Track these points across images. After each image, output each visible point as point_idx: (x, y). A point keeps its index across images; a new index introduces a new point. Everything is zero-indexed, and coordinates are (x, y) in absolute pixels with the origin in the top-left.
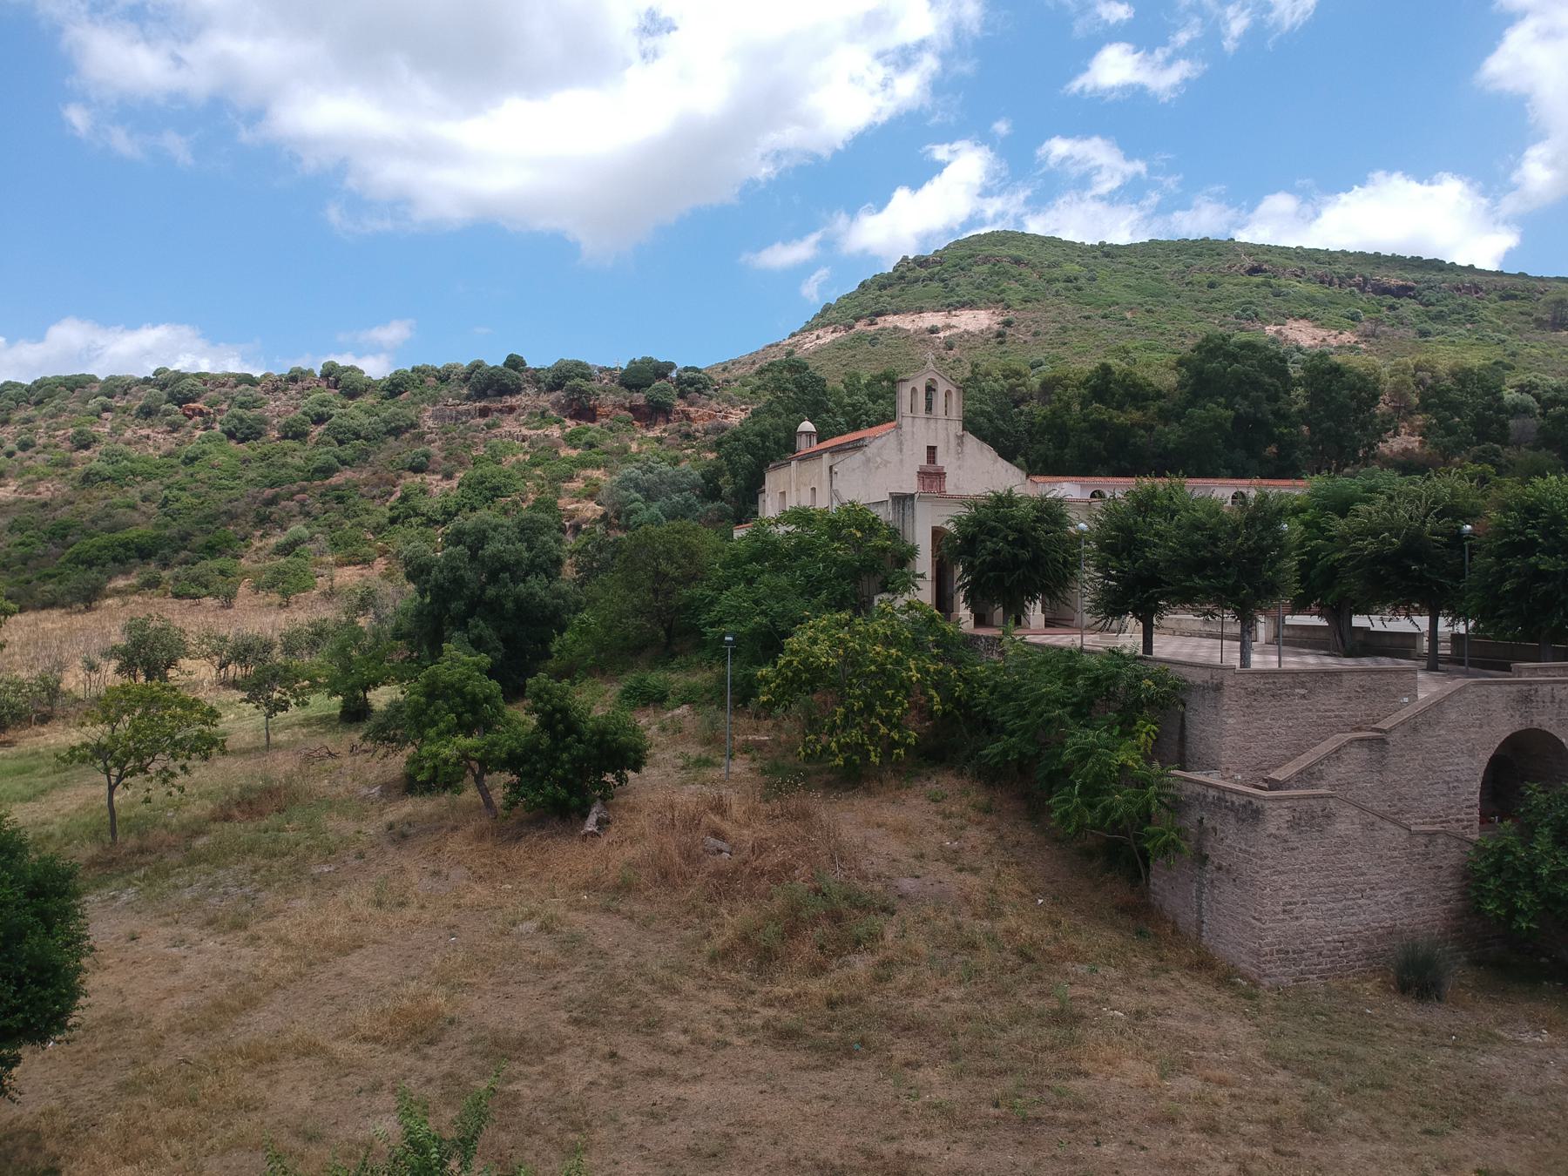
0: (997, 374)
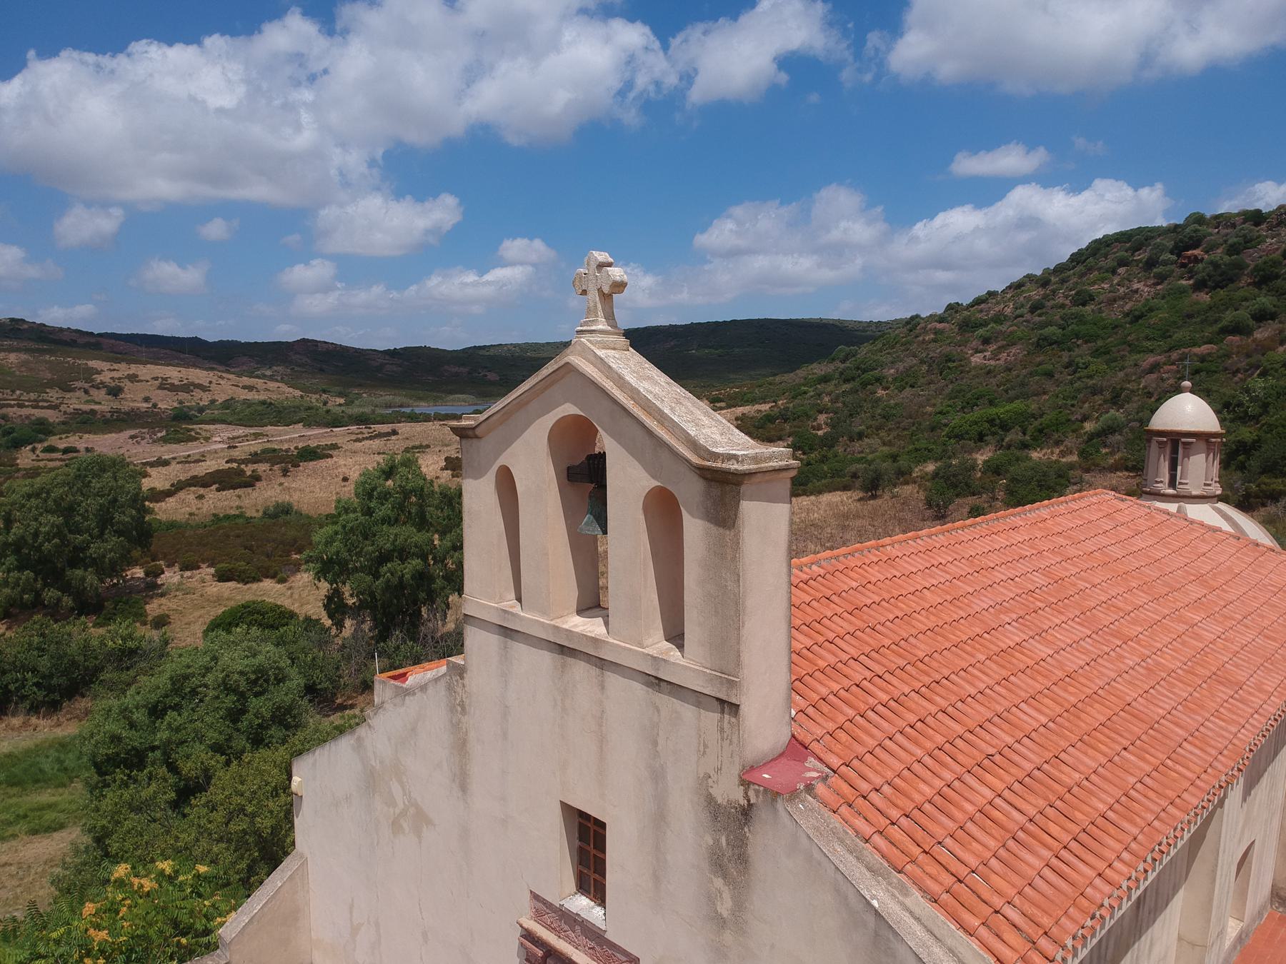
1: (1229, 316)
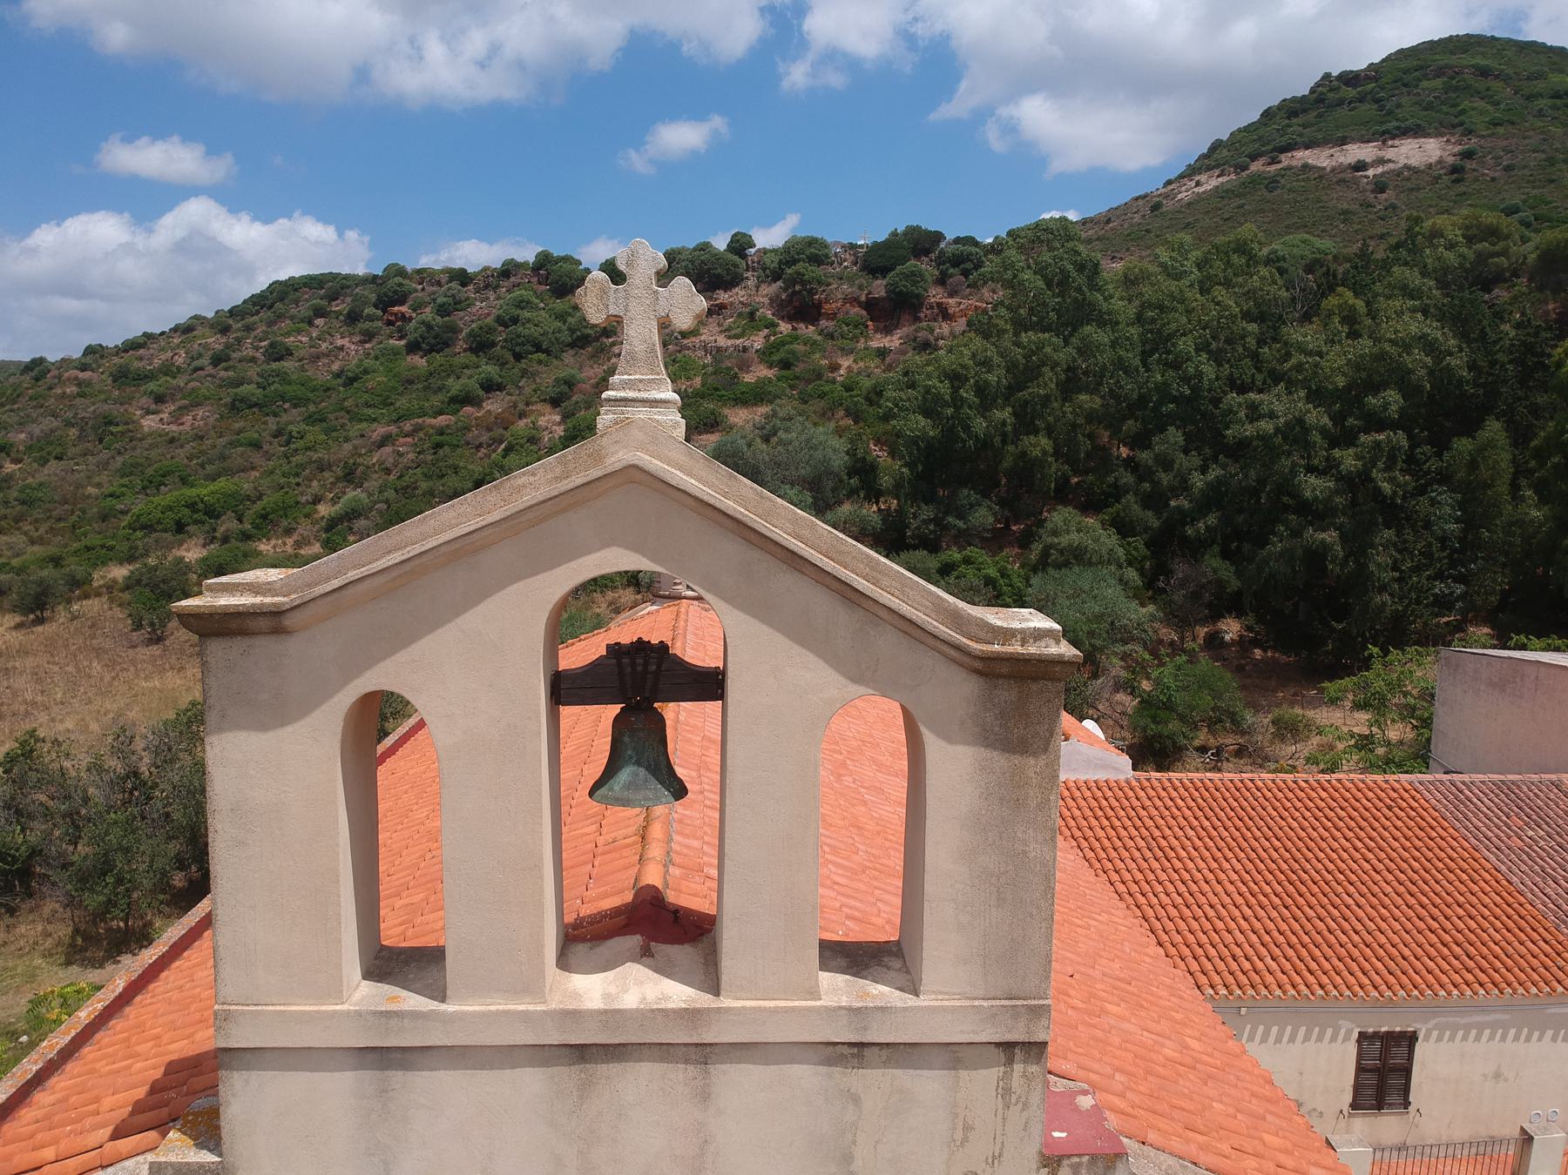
0: (1455, 234)
1: (455, 386)
